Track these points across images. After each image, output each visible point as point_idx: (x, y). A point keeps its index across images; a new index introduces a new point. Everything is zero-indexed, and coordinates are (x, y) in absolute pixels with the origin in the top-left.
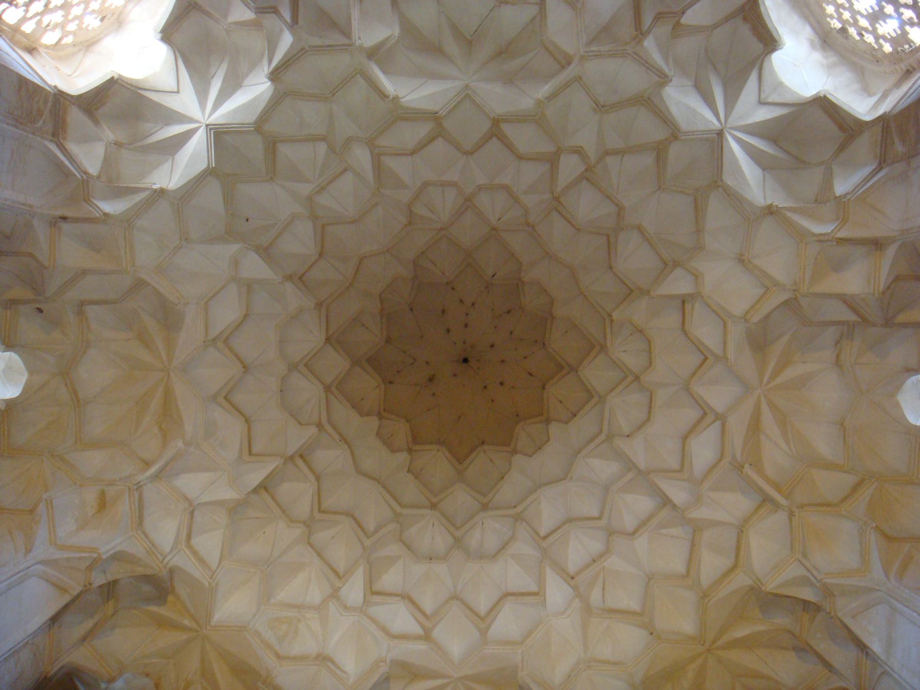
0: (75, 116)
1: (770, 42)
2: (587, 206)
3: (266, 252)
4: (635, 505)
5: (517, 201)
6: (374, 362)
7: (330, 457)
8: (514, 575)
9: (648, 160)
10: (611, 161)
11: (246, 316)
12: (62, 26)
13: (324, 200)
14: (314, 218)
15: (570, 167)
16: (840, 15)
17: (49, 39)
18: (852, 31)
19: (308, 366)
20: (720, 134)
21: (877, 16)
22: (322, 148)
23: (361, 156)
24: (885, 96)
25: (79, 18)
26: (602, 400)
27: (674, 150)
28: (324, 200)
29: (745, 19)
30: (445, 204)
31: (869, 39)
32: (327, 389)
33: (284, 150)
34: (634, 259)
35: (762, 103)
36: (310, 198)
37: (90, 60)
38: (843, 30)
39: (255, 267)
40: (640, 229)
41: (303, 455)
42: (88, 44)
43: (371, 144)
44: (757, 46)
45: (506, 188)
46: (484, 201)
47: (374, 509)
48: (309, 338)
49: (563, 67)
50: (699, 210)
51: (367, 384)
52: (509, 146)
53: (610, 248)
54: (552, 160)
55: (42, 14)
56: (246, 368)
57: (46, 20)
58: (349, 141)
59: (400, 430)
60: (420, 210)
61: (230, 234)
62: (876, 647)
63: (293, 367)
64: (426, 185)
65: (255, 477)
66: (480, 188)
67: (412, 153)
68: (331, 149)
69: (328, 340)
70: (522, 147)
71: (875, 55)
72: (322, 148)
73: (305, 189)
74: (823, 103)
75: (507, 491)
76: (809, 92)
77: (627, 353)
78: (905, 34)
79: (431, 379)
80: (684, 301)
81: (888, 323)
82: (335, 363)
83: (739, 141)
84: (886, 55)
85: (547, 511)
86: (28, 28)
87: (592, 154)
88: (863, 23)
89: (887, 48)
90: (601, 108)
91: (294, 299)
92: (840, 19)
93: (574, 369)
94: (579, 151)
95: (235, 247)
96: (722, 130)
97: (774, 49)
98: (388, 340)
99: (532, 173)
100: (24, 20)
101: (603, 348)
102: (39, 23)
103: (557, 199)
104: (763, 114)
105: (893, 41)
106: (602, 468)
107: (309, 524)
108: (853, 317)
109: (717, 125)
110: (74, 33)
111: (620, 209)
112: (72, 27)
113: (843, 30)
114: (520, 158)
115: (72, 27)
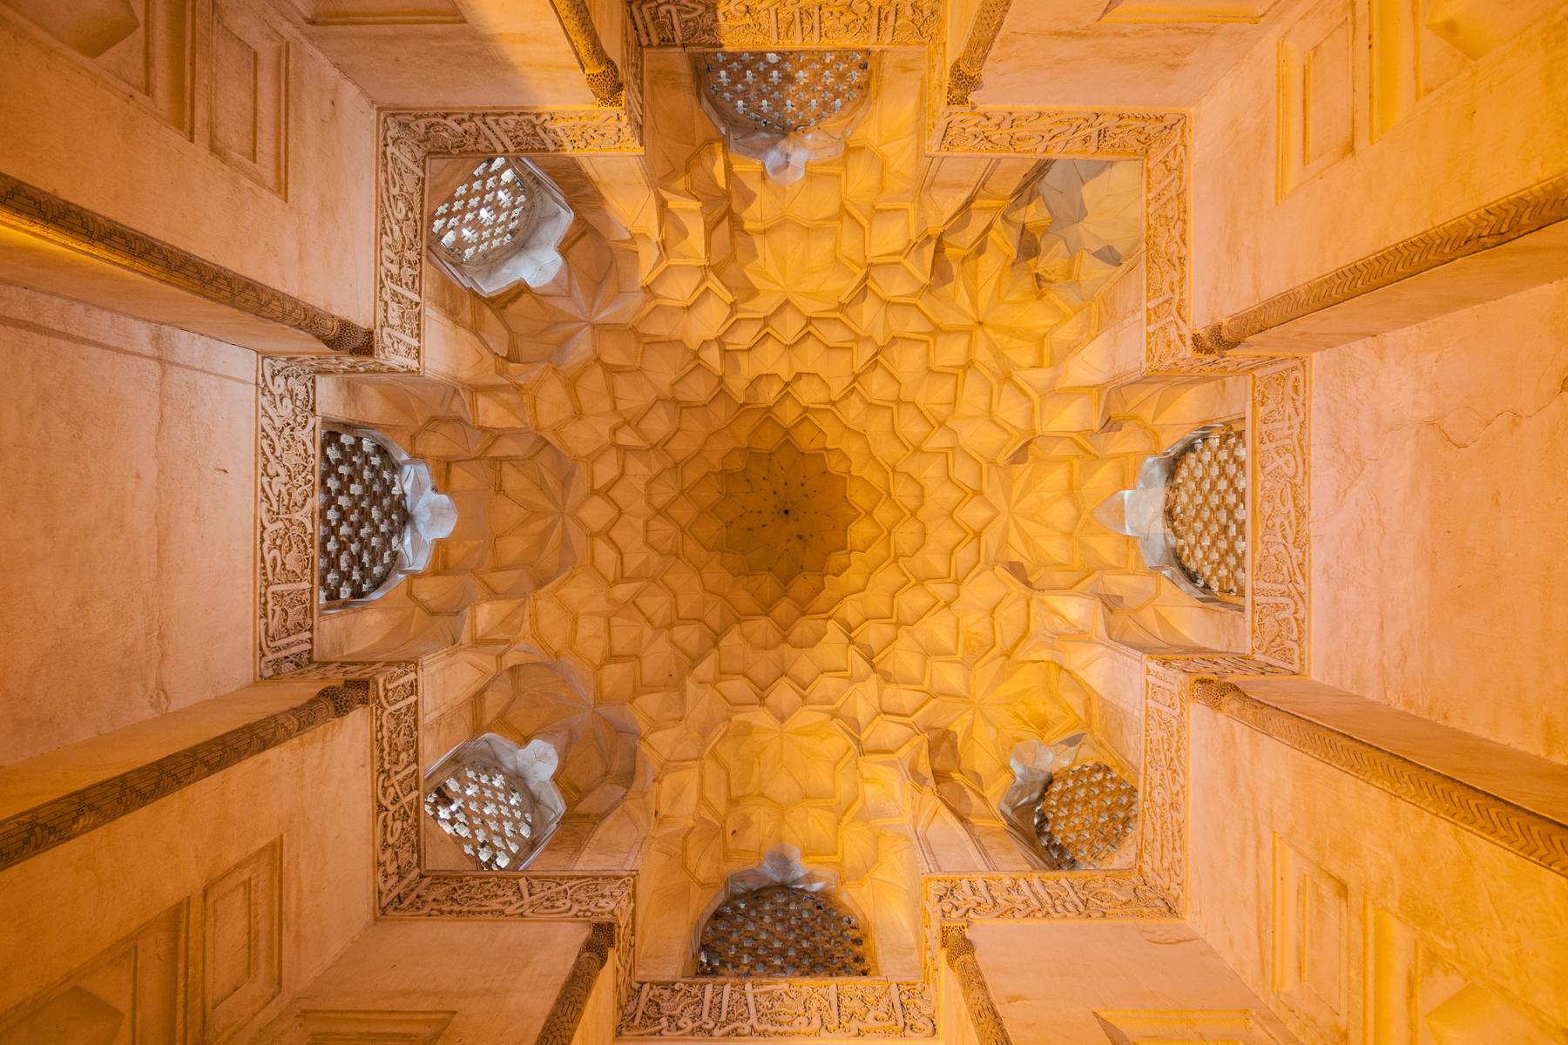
0: (581, 808)
1: (521, 289)
2: (658, 425)
3: (695, 662)
4: (878, 386)
5: (657, 476)
6: (786, 581)
7: (850, 610)
8: (931, 472)
9: (621, 382)
10: (621, 406)
11: (744, 675)
12: (516, 823)
13: (658, 619)
14: (671, 626)
15: (627, 438)
16: (500, 235)
17: (525, 832)
18: (512, 226)
19: (785, 630)
20: (594, 326)
21: (496, 208)
22: (616, 621)
23: (623, 591)
24: (557, 201)
25: (511, 808)
26: (806, 409)
27: (609, 359)
28: (658, 619)
29: (504, 307)
30: (663, 530)
31: (517, 211)
32: (803, 614)
33: (618, 649)
34: (698, 390)
35: (569, 295)
36: (655, 629)
37: (546, 799)
38: (511, 232)
39: (705, 669)
40: (673, 385)
41: (849, 629)
42: (533, 801)
43: (615, 583)
44: (525, 298)
45: (648, 484)
46: (660, 500)
47: (888, 576)
48: (762, 628)
49: (548, 443)
50: (655, 342)
51: (800, 586)
52: (614, 483)
53: (690, 406)
54: (624, 450)
55: (504, 838)
56: (784, 674)
57: (509, 834)
58: (608, 600)
59: (837, 559)
60: (667, 547)
61: (680, 688)
62: (963, 196)
63: (785, 639)
64: (646, 542)
65: (861, 666)
66: (649, 503)
67: (621, 554)
68: (616, 613)
69: (767, 614)
70: (613, 473)
71: (529, 209)
72: (616, 621)
73: (648, 632)
74: (564, 249)
75: (876, 479)
76: (560, 259)
77: (770, 393)
78: (507, 186)
79: (800, 537)
80: (725, 352)
81: (727, 195)
82: (783, 609)
83: (598, 312)
84: (528, 200)
85: (887, 451)
86: (514, 848)
87: (616, 420)
88: (503, 218)
89: (522, 199)
90: (579, 415)
91: (732, 639)
92: (503, 235)
93: (787, 431)
94: (614, 430)
95: (690, 685)
96: (594, 326)
97: (526, 285)
98: (770, 570)
99: (635, 466)
100: (508, 852)
101: (768, 409)
102: (511, 839)
103: (653, 447)
104: (578, 294)
105: (515, 194)
106: (853, 411)
107: (898, 625)
108: (726, 222)
109: (588, 328)
110: (523, 813)
111: (658, 400)
112: (518, 814)
113: (511, 232)
114: (622, 474)
115: (518, 814)
